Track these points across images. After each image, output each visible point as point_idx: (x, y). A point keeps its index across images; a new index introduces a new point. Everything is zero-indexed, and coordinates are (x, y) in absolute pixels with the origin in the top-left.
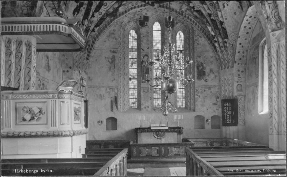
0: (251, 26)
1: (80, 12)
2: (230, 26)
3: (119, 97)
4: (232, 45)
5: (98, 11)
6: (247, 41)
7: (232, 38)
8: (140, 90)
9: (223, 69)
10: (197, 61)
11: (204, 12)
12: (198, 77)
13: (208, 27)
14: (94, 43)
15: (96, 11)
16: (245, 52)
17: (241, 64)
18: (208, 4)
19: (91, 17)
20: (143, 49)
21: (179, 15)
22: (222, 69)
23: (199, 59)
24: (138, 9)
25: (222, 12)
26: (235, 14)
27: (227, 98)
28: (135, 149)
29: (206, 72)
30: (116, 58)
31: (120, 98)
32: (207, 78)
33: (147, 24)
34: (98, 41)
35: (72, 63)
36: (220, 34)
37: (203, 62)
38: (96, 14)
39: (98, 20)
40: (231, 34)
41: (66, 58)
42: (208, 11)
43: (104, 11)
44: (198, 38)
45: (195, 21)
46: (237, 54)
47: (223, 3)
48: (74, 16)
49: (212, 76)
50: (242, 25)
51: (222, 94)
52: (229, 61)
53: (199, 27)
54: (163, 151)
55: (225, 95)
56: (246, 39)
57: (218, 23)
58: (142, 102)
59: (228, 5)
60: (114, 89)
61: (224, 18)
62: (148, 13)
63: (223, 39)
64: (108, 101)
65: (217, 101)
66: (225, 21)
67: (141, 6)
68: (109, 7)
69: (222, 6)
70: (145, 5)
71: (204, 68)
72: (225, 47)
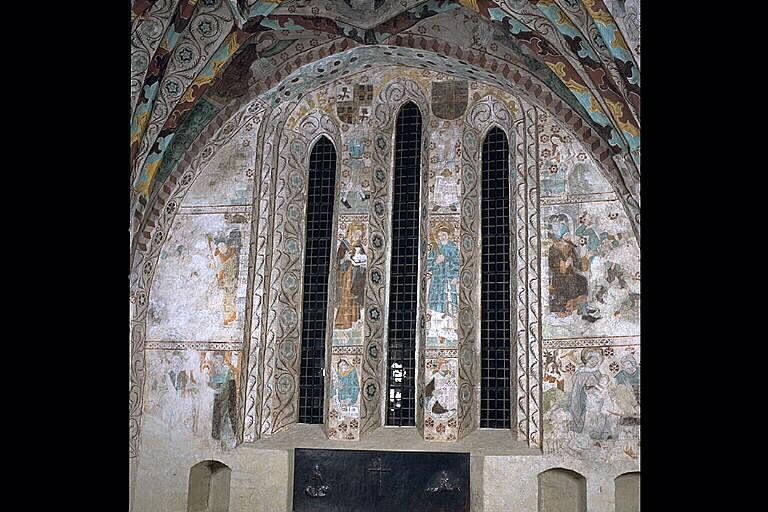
11: (551, 38)
12: (556, 300)
20: (346, 203)
23: (557, 229)
24: (325, 62)
30: (246, 242)
32: (598, 305)
33: (365, 111)
37: (575, 240)
44: (555, 146)
45: (534, 81)
62: (369, 72)
67: (332, 51)
68: (202, 63)
70: (344, 47)
71: (580, 264)
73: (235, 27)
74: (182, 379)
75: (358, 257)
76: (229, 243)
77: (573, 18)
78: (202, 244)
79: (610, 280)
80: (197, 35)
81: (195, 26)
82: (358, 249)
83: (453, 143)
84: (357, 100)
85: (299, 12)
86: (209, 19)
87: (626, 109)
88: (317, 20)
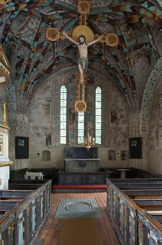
0: (156, 78)
1: (22, 67)
2: (139, 80)
3: (53, 135)
4: (138, 96)
5: (37, 67)
6: (152, 91)
7: (139, 90)
8: (68, 131)
9: (131, 115)
10: (111, 109)
11: (118, 69)
13: (121, 81)
14: (34, 93)
15: (34, 67)
16: (149, 101)
17: (146, 110)
18: (122, 62)
19: (31, 72)
21: (98, 73)
22: (130, 115)
25: (133, 68)
26: (143, 69)
27: (133, 137)
28: (62, 177)
29: (118, 117)
30: (51, 106)
31: (53, 136)
32: (119, 122)
33: (74, 80)
34: (37, 92)
35: (16, 108)
36: (130, 87)
37: (115, 110)
38: (34, 69)
39: (37, 75)
40: (138, 86)
41: (12, 104)
42: (121, 68)
43: (41, 67)
45: (110, 78)
46: (143, 102)
47: (134, 60)
48: (16, 69)
49: (122, 120)
50: (149, 77)
51: (129, 134)
52: (136, 108)
53: (113, 82)
54: (85, 179)
55: (132, 135)
56: (151, 90)
57: (128, 78)
58: (70, 139)
59: (137, 62)
60: (49, 129)
61: (134, 73)
62: (75, 72)
63: (131, 90)
64: (44, 138)
65: (125, 139)
66: (134, 76)
67: (70, 66)
68: (45, 65)
69: (133, 63)
70: (73, 65)
71: (116, 114)
72: (133, 97)
73: (54, 57)
74: (38, 134)
75: (73, 111)
76: (47, 106)
77: (123, 66)
78: (41, 106)
79: (121, 117)
80: (45, 58)
81: (45, 56)
82: (73, 109)
83: (92, 89)
84: (72, 78)
85: (66, 56)
86: (49, 54)
87: (129, 85)
88: (69, 58)
